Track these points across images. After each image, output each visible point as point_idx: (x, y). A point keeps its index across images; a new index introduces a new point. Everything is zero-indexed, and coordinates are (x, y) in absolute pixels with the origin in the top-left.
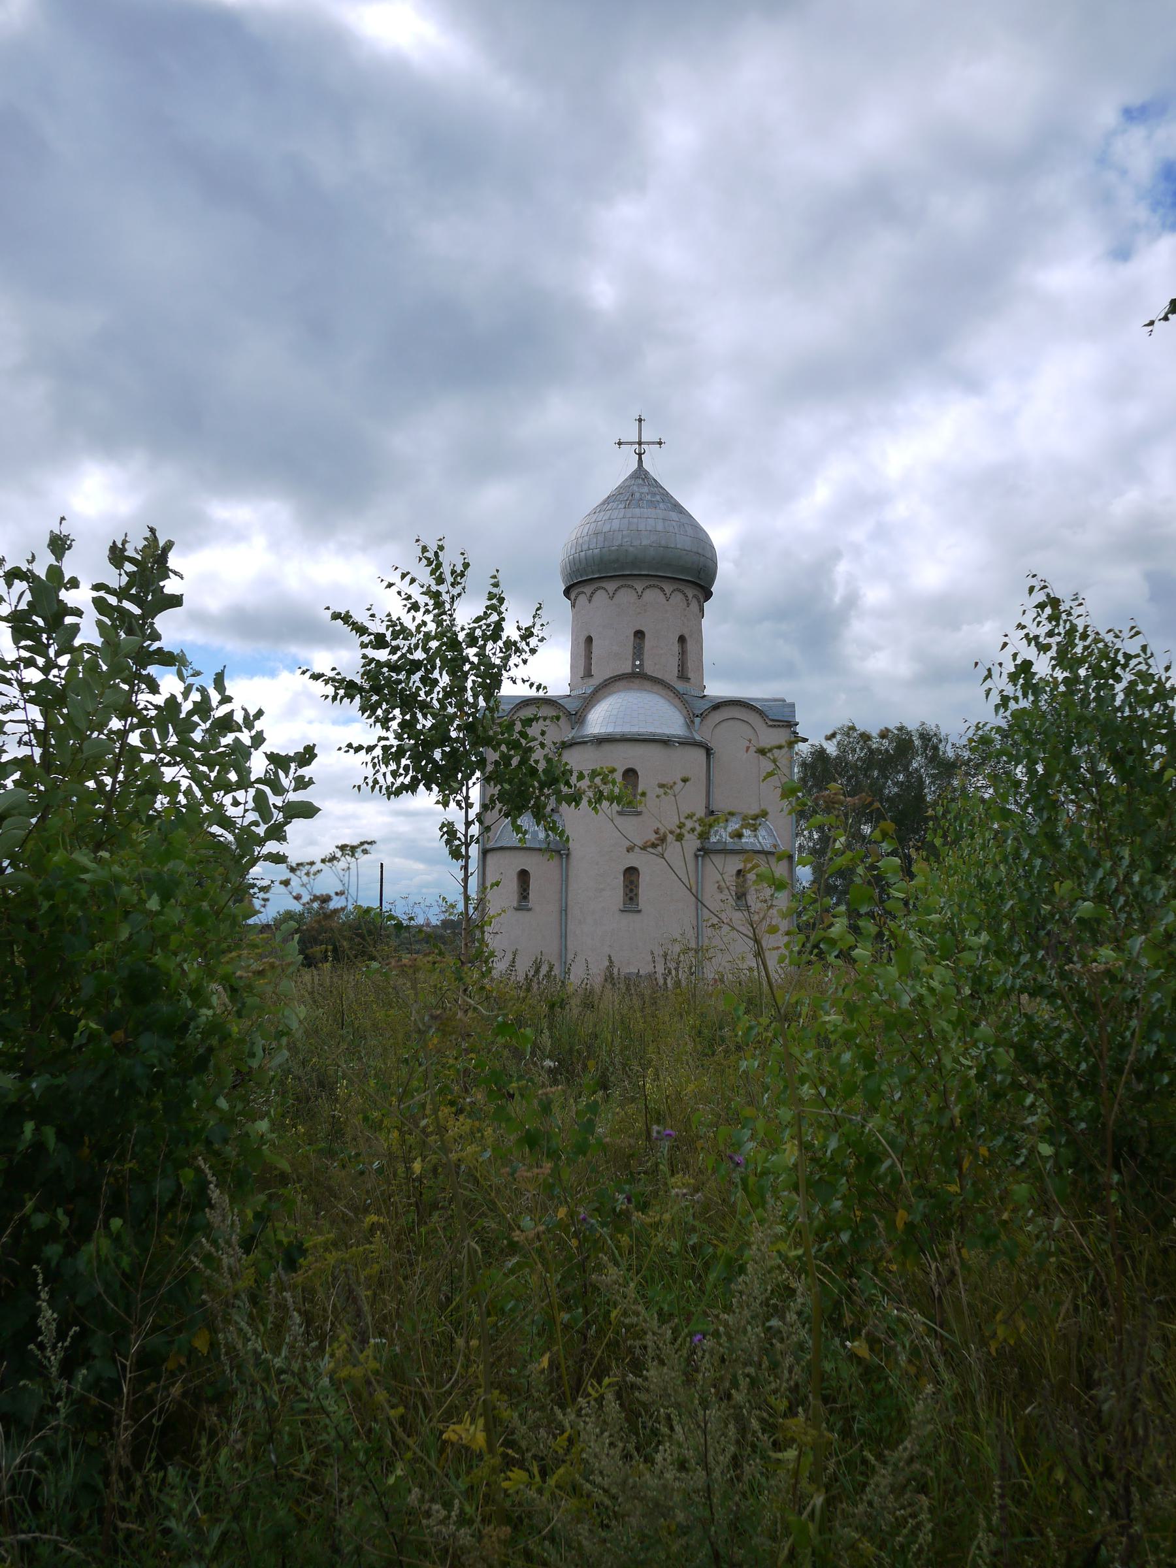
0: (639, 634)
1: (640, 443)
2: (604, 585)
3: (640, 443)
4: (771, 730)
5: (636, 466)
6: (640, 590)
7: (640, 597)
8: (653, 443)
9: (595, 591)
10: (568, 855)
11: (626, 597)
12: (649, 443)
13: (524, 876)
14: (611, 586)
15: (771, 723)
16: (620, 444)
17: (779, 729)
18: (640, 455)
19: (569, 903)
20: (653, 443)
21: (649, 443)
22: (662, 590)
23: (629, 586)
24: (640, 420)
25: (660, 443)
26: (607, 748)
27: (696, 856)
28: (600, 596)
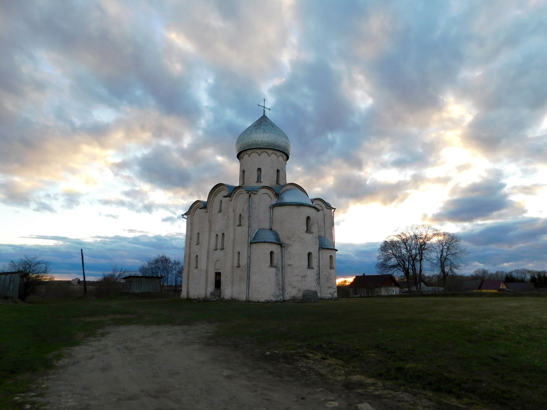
0: (278, 171)
1: (264, 107)
4: (327, 210)
5: (263, 115)
6: (278, 155)
7: (278, 158)
9: (262, 152)
11: (274, 157)
13: (272, 253)
14: (270, 152)
15: (328, 207)
18: (264, 111)
22: (283, 157)
24: (265, 100)
26: (302, 209)
27: (319, 250)
28: (264, 155)
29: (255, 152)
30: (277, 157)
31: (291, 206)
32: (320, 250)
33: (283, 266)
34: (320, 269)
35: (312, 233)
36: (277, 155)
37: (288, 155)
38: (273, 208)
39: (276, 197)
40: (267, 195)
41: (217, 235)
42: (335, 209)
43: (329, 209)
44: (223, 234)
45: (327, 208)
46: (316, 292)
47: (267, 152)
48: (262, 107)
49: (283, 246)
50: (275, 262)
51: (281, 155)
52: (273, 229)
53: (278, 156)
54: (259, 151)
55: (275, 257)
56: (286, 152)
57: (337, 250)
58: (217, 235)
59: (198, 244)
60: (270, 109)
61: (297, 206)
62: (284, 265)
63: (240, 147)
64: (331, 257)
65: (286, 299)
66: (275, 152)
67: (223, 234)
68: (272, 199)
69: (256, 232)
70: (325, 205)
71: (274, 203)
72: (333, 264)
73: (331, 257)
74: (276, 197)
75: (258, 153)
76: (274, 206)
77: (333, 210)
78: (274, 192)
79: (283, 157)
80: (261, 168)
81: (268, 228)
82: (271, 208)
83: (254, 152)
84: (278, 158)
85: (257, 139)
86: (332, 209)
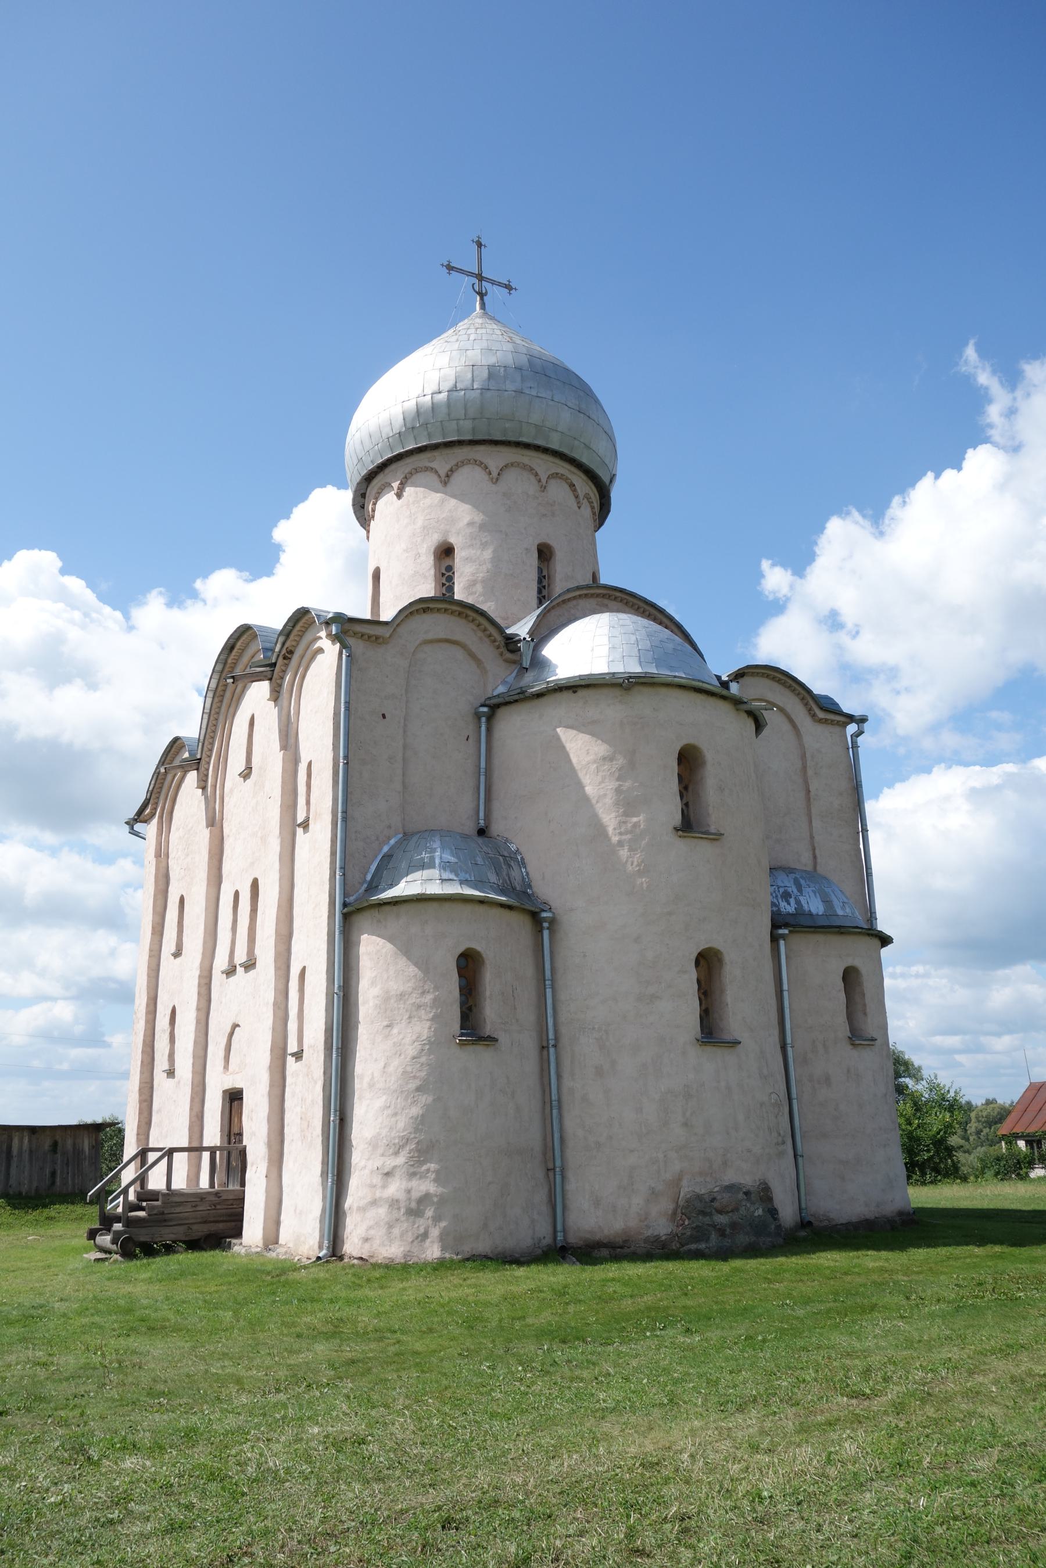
1: (480, 277)
2: (480, 453)
3: (480, 277)
7: (544, 488)
8: (499, 284)
10: (553, 921)
12: (493, 282)
14: (495, 458)
15: (821, 715)
16: (450, 268)
17: (831, 728)
19: (563, 1030)
20: (499, 284)
21: (493, 282)
22: (572, 486)
23: (525, 467)
24: (480, 245)
25: (508, 287)
27: (774, 939)
29: (427, 469)
30: (532, 488)
31: (581, 693)
32: (783, 937)
33: (551, 1036)
34: (790, 1050)
35: (717, 837)
36: (536, 475)
37: (606, 479)
38: (490, 718)
39: (506, 661)
40: (459, 654)
41: (237, 894)
42: (862, 720)
43: (825, 721)
44: (255, 885)
45: (821, 721)
46: (765, 1193)
47: (481, 464)
48: (470, 274)
49: (545, 919)
50: (491, 1012)
51: (555, 476)
52: (498, 828)
53: (540, 481)
54: (441, 462)
55: (491, 983)
56: (585, 460)
57: (885, 940)
58: (237, 894)
59: (177, 954)
60: (513, 285)
61: (617, 692)
62: (556, 1031)
63: (356, 462)
64: (850, 977)
65: (572, 1239)
66: (526, 460)
67: (255, 885)
68: (484, 671)
69: (386, 849)
70: (806, 704)
71: (501, 689)
72: (865, 1014)
73: (850, 977)
74: (509, 655)
75: (436, 472)
76: (498, 706)
77: (852, 728)
78: (499, 638)
79: (572, 486)
80: (452, 540)
81: (470, 828)
82: (478, 716)
83: (417, 471)
84: (544, 488)
85: (429, 398)
86: (844, 725)
